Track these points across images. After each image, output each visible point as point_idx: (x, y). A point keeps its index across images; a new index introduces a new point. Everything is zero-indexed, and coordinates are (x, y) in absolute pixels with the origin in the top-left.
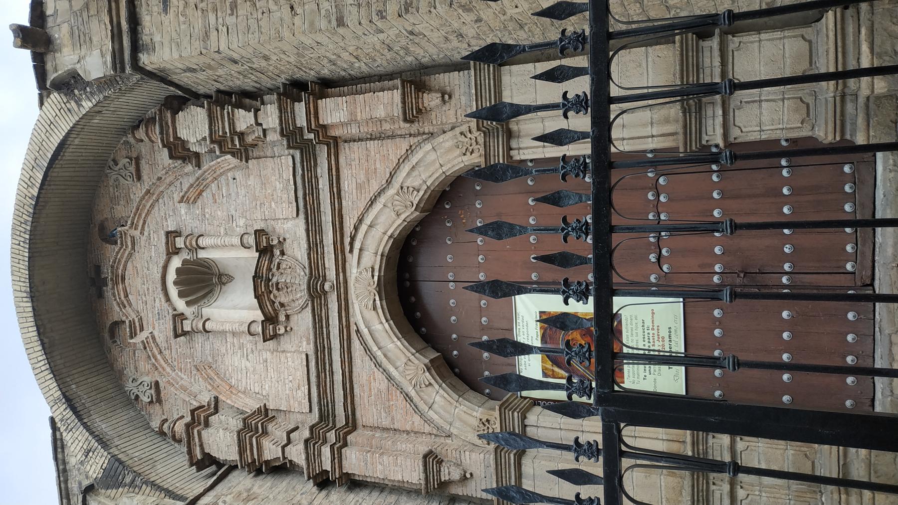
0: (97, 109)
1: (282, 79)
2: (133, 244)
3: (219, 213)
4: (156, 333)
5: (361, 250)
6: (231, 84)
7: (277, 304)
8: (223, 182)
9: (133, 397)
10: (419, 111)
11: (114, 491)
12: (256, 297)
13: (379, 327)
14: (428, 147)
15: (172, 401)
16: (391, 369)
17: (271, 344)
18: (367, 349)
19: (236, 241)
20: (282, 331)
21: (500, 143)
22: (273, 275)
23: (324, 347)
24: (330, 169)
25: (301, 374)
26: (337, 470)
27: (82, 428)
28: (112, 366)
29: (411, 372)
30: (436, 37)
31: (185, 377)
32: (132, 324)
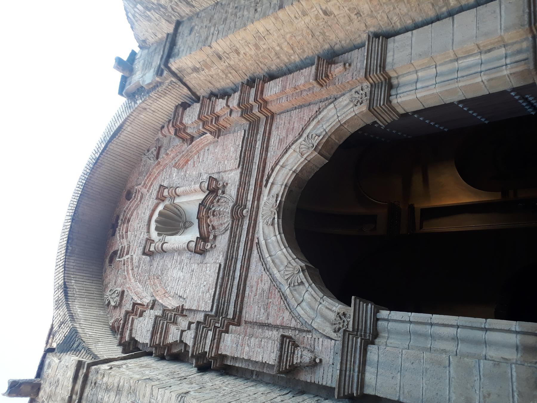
0: (144, 105)
2: (142, 198)
3: (194, 173)
4: (134, 256)
5: (273, 184)
7: (211, 227)
8: (202, 153)
9: (107, 302)
10: (327, 76)
12: (197, 218)
13: (274, 238)
14: (332, 106)
16: (275, 271)
18: (261, 257)
19: (197, 186)
21: (383, 90)
22: (213, 206)
23: (232, 257)
25: (212, 279)
26: (214, 350)
28: (103, 281)
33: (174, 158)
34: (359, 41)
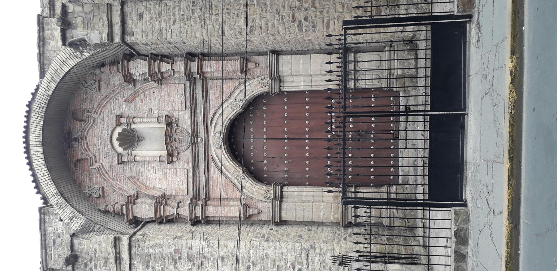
1: (184, 52)
2: (94, 121)
4: (104, 164)
6: (160, 51)
8: (147, 92)
9: (88, 196)
11: (88, 235)
15: (111, 196)
16: (227, 173)
17: (170, 165)
18: (217, 166)
20: (176, 159)
24: (203, 90)
25: (184, 178)
27: (70, 206)
28: (75, 181)
29: (236, 174)
30: (257, 43)
31: (120, 184)
32: (91, 159)
33: (119, 93)
34: (262, 50)
